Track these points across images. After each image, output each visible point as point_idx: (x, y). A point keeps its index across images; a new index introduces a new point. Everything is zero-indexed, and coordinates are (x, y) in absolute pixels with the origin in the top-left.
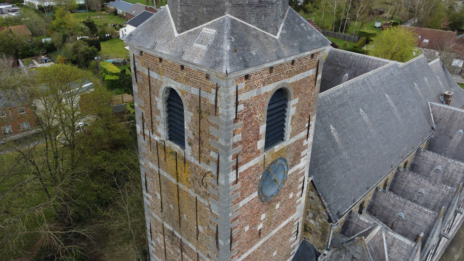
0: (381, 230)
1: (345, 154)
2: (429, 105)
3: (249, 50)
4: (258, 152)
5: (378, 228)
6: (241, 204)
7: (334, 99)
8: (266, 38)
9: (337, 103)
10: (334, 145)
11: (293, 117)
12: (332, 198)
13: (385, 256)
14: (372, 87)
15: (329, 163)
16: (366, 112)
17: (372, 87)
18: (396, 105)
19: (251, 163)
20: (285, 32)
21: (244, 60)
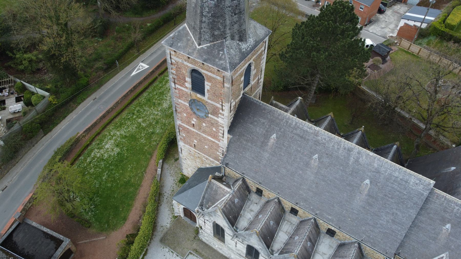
0: (229, 192)
1: (266, 155)
2: (441, 256)
3: (179, 42)
4: (186, 87)
5: (229, 190)
6: (180, 101)
7: (299, 128)
8: (192, 44)
9: (298, 131)
10: (264, 144)
11: (208, 91)
12: (232, 156)
13: (218, 200)
14: (357, 161)
15: (249, 144)
16: (321, 162)
17: (357, 161)
18: (369, 195)
19: (183, 89)
20: (206, 48)
21: (172, 44)
